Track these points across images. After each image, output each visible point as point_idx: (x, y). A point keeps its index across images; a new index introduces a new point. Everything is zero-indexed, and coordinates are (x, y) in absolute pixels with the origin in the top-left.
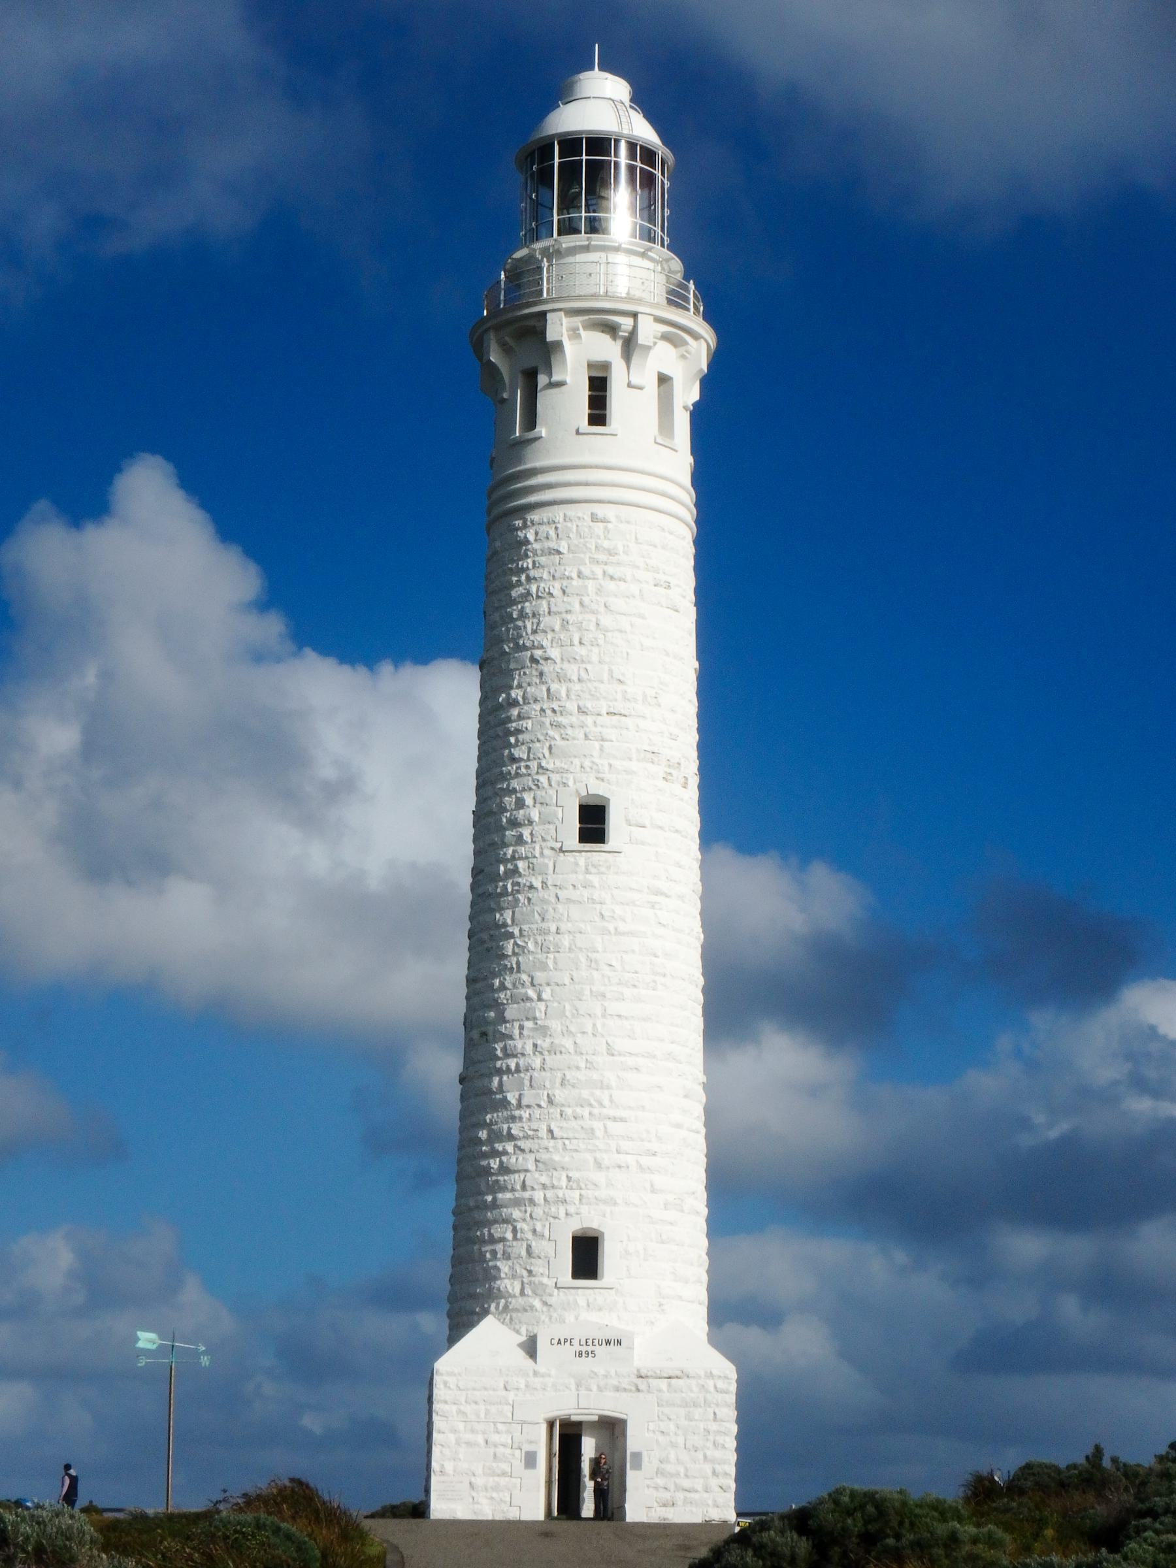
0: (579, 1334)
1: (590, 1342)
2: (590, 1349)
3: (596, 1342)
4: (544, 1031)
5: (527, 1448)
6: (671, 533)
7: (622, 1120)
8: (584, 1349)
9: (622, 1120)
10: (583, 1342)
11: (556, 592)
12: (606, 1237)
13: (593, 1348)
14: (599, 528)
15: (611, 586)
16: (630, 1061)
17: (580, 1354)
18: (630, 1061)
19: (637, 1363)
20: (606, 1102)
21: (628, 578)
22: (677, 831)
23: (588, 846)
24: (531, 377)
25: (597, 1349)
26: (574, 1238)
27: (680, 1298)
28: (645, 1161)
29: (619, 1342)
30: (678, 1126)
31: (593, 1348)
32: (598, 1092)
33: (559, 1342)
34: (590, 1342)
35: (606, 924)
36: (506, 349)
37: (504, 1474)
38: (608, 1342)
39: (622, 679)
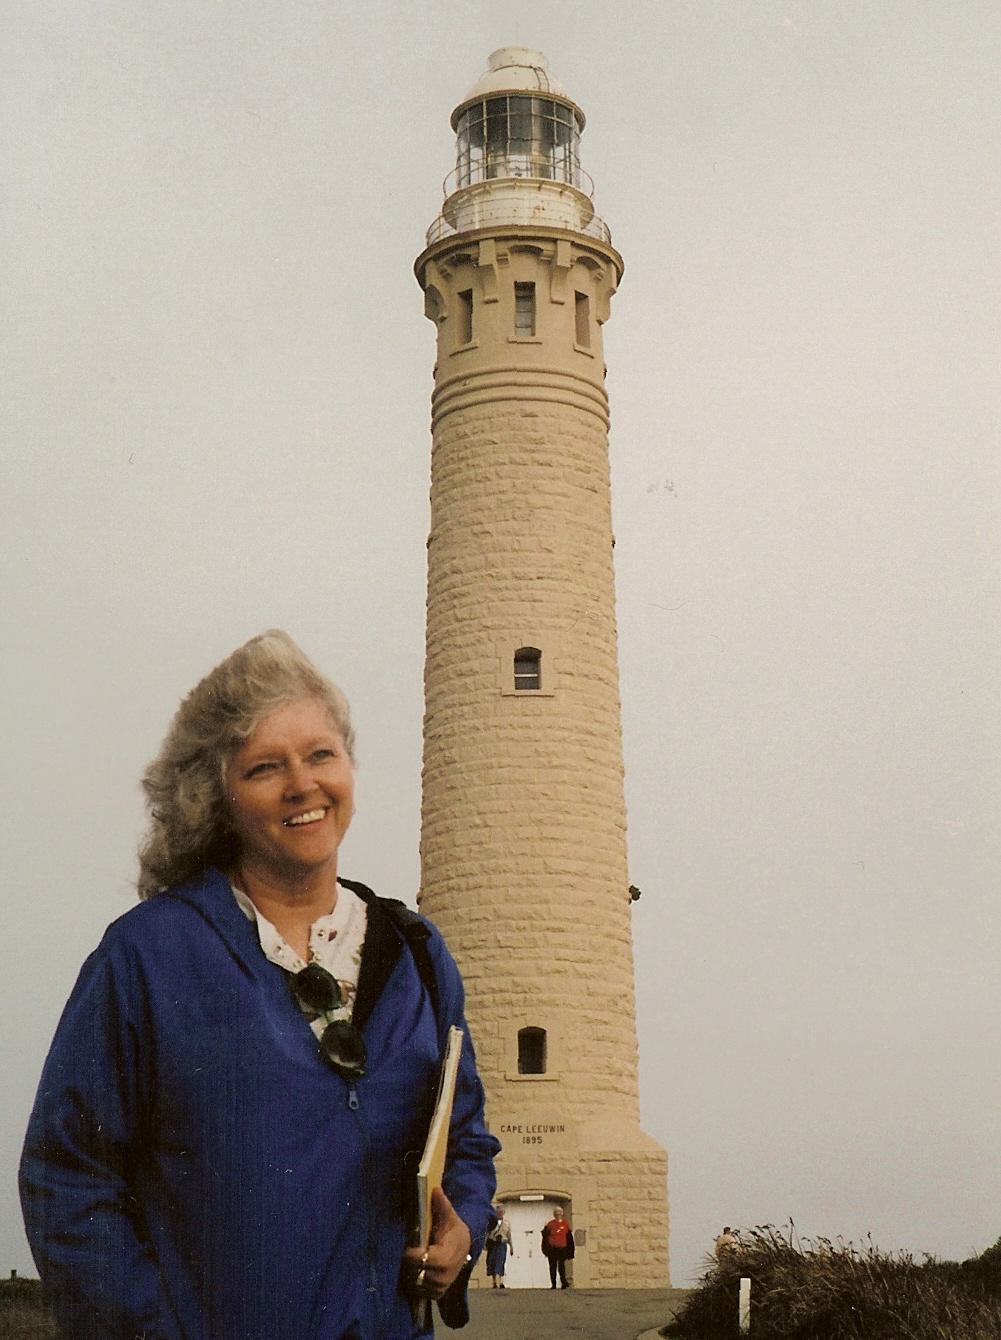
2: (536, 1135)
3: (542, 1128)
4: (492, 854)
7: (561, 930)
8: (531, 1135)
9: (561, 930)
10: (530, 1129)
11: (493, 477)
13: (539, 1134)
15: (541, 470)
16: (566, 879)
18: (566, 879)
22: (600, 679)
24: (467, 296)
28: (581, 968)
29: (563, 1130)
30: (609, 936)
31: (539, 1134)
32: (538, 907)
34: (536, 1130)
35: (542, 759)
36: (446, 276)
39: (549, 548)
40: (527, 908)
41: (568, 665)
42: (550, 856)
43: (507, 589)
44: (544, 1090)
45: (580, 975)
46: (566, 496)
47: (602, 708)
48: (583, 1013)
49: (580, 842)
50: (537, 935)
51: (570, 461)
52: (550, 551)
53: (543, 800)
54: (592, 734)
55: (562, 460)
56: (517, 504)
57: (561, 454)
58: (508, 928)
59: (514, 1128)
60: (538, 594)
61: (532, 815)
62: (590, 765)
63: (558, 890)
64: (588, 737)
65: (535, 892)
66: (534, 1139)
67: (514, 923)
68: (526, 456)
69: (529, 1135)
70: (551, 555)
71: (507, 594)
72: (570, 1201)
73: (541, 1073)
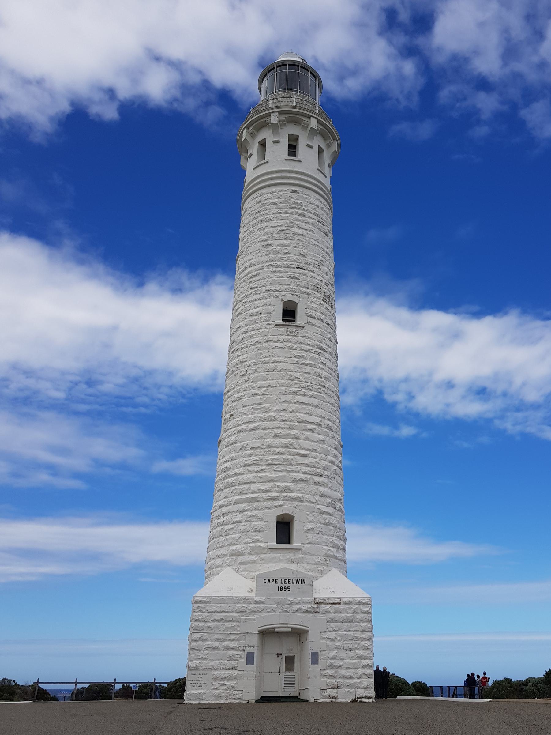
0: (280, 576)
1: (287, 581)
3: (291, 581)
5: (248, 650)
6: (324, 205)
7: (304, 455)
8: (283, 585)
9: (304, 455)
10: (283, 581)
12: (295, 519)
13: (289, 585)
14: (294, 195)
17: (281, 590)
19: (315, 595)
20: (296, 446)
21: (307, 216)
22: (329, 324)
23: (287, 323)
25: (291, 585)
26: (278, 523)
27: (335, 557)
28: (317, 479)
29: (304, 582)
30: (332, 462)
31: (289, 585)
32: (292, 441)
33: (269, 582)
34: (287, 581)
35: (295, 359)
37: (234, 668)
38: (298, 582)
40: (286, 441)
41: (313, 313)
42: (300, 412)
43: (279, 272)
44: (291, 555)
45: (317, 483)
46: (313, 232)
47: (329, 339)
48: (318, 507)
49: (317, 406)
50: (290, 457)
51: (315, 217)
52: (304, 256)
53: (296, 381)
54: (323, 350)
55: (310, 215)
56: (288, 231)
57: (311, 213)
58: (274, 453)
59: (273, 580)
60: (297, 275)
61: (290, 389)
62: (322, 366)
63: (304, 432)
64: (321, 352)
65: (289, 432)
66: (285, 588)
67: (278, 450)
68: (292, 210)
69: (282, 585)
70: (305, 258)
71: (279, 274)
72: (307, 632)
73: (289, 543)
